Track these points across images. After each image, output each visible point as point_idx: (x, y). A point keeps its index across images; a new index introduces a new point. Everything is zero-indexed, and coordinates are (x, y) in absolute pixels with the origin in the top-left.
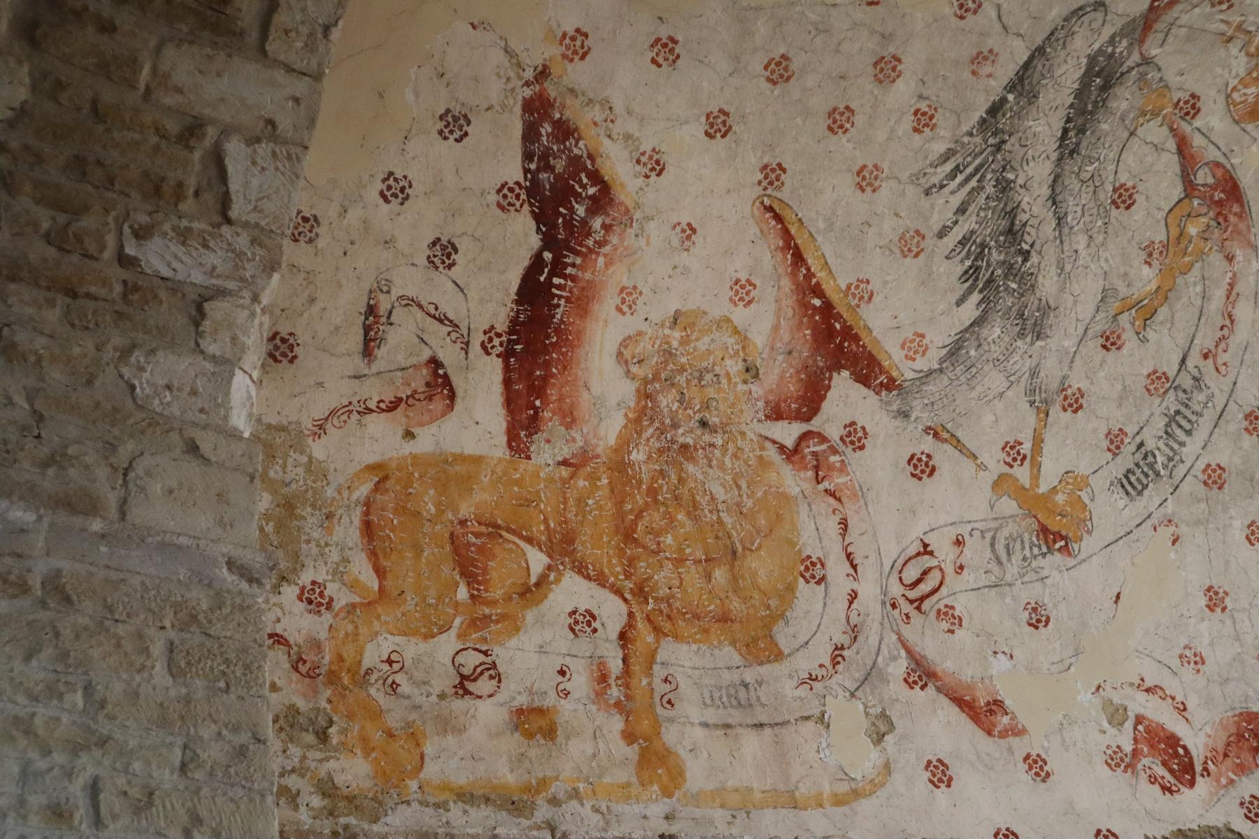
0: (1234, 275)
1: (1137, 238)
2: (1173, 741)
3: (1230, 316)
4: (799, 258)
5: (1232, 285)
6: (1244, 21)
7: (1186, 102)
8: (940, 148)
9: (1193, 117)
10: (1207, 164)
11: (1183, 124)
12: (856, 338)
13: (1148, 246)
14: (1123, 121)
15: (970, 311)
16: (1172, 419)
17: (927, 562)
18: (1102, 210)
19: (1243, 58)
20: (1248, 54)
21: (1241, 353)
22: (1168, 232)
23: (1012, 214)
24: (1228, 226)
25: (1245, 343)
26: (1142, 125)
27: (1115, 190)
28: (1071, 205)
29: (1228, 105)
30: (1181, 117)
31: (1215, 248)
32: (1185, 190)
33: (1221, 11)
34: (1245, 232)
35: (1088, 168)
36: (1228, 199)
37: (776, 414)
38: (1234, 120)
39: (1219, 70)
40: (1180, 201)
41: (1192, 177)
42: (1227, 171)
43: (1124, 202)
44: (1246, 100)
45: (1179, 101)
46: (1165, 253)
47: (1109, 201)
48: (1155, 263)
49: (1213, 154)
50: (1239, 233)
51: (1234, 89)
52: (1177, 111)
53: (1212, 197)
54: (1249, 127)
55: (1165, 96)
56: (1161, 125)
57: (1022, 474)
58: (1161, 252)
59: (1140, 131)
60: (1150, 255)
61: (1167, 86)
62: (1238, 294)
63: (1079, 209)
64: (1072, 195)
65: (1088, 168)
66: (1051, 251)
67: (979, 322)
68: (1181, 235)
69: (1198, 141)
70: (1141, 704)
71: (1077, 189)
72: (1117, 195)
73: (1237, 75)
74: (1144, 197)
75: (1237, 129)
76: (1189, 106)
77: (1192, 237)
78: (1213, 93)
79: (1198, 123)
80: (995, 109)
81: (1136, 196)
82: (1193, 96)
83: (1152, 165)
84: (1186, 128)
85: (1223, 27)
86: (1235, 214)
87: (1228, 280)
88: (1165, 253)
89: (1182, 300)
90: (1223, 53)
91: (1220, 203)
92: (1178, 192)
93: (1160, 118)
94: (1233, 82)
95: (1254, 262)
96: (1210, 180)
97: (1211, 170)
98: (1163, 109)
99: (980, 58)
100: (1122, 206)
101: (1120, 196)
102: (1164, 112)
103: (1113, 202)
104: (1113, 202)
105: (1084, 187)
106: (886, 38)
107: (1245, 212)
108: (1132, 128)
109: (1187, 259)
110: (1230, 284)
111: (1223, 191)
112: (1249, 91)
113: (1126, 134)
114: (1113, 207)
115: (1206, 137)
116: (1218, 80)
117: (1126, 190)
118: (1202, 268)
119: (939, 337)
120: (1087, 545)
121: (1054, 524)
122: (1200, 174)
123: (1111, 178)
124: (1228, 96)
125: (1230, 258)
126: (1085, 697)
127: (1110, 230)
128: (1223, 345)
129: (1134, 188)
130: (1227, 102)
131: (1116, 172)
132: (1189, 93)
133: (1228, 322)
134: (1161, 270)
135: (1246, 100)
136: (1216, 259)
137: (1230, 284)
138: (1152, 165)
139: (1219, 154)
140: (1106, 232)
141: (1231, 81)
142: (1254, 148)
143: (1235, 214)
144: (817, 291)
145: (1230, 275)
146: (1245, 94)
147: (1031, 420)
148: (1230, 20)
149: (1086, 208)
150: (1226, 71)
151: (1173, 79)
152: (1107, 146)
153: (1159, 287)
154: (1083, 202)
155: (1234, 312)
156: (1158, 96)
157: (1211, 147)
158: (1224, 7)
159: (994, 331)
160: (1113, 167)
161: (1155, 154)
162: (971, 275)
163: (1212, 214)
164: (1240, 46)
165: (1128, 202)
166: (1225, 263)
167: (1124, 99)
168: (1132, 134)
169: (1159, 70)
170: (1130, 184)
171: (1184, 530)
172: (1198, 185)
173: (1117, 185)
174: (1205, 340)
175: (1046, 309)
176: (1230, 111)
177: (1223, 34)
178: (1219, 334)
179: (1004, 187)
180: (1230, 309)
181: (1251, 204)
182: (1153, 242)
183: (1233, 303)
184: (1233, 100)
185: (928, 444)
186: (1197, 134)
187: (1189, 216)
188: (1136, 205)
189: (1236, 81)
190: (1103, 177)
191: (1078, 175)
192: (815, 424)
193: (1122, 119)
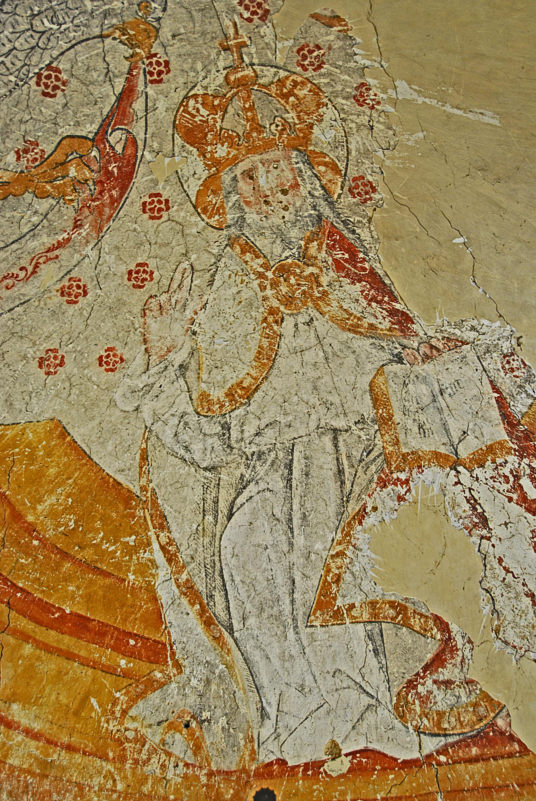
0: (69, 240)
1: (29, 126)
3: (36, 266)
5: (60, 245)
6: (247, 46)
7: (158, 63)
9: (152, 82)
10: (128, 132)
11: (142, 77)
13: (31, 143)
14: (105, 17)
18: (24, 70)
19: (221, 80)
20: (226, 78)
21: (17, 303)
22: (55, 150)
24: (98, 199)
25: (27, 298)
26: (114, 39)
27: (49, 67)
29: (181, 104)
30: (145, 69)
31: (75, 204)
32: (96, 134)
33: (241, 15)
34: (105, 217)
35: (45, 21)
36: (116, 179)
38: (175, 121)
39: (199, 66)
40: (86, 138)
41: (110, 131)
42: (136, 157)
43: (47, 86)
44: (194, 116)
45: (155, 55)
46: (37, 163)
47: (37, 71)
48: (23, 161)
49: (138, 130)
50: (101, 214)
51: (195, 96)
52: (147, 62)
53: (109, 162)
54: (179, 141)
55: (149, 37)
56: (126, 58)
58: (36, 159)
59: (108, 41)
60: (26, 151)
61: (157, 30)
62: (57, 257)
63: (9, 46)
64: (13, 27)
65: (45, 21)
68: (62, 164)
69: (138, 105)
71: (22, 28)
72: (46, 73)
73: (206, 88)
74: (65, 101)
75: (170, 132)
76: (157, 69)
77: (67, 176)
78: (181, 80)
79: (150, 90)
81: (59, 92)
82: (167, 63)
83: (92, 83)
84: (140, 87)
85: (231, 31)
86: (111, 196)
87: (60, 238)
88: (37, 163)
89: (15, 213)
90: (213, 56)
91: (109, 174)
93: (131, 51)
94: (199, 90)
95: (90, 247)
96: (119, 148)
97: (127, 139)
98: (139, 47)
100: (43, 87)
101: (48, 77)
102: (138, 51)
103: (39, 75)
104: (39, 75)
105: (28, 34)
107: (120, 203)
108: (105, 32)
109: (48, 187)
110: (59, 242)
111: (119, 168)
112: (203, 112)
113: (97, 31)
114: (35, 79)
115: (146, 110)
116: (192, 74)
117: (57, 79)
118: (52, 208)
122: (118, 134)
123: (55, 53)
124: (186, 97)
125: (77, 225)
127: (15, 94)
128: (10, 282)
129: (64, 84)
130: (183, 101)
131: (62, 54)
132: (167, 59)
133: (30, 269)
134: (22, 172)
135: (194, 116)
136: (69, 212)
137: (59, 242)
138: (92, 83)
139: (142, 136)
140: (10, 91)
141: (199, 87)
142: (167, 160)
143: (111, 196)
145: (65, 236)
146: (198, 111)
148: (240, 32)
149: (14, 51)
150: (203, 74)
151: (166, 33)
152: (76, 22)
153: (9, 183)
154: (17, 45)
155: (42, 266)
156: (145, 30)
157: (142, 122)
158: (246, 15)
160: (66, 46)
161: (102, 78)
163: (95, 175)
164: (228, 63)
165: (49, 90)
166: (71, 223)
168: (101, 37)
169: (164, 10)
170: (64, 76)
172: (108, 142)
173: (54, 65)
176: (178, 111)
177: (227, 38)
178: (16, 271)
180: (41, 261)
181: (127, 202)
182: (37, 145)
183: (49, 259)
184: (187, 105)
186: (142, 99)
187: (81, 157)
188: (52, 100)
189: (201, 92)
190: (50, 44)
191: (33, 16)
193: (106, 14)
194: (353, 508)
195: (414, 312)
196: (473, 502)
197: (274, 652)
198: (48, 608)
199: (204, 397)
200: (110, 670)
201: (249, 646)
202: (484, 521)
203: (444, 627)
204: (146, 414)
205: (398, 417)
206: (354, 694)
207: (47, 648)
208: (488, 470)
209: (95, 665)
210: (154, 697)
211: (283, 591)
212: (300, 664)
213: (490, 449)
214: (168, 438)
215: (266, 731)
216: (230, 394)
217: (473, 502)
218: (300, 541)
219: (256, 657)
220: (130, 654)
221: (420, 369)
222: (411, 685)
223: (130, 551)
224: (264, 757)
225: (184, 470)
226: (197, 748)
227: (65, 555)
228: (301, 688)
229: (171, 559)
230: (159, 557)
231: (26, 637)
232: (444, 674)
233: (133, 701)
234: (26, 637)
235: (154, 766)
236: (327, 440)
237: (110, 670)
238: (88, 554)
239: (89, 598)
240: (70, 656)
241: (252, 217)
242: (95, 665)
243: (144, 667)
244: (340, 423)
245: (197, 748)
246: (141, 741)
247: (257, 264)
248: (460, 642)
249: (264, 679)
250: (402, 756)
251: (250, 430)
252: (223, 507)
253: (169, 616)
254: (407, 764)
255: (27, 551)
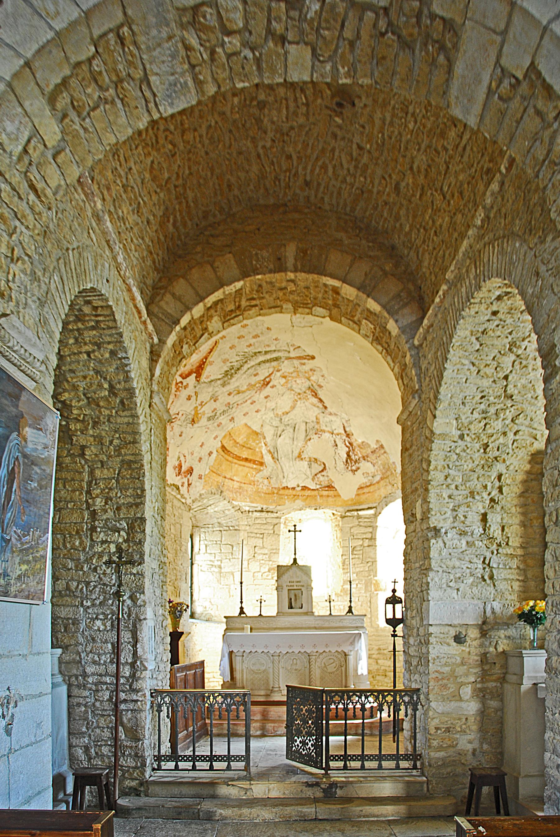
2: (181, 467)
4: (210, 353)
8: (246, 350)
12: (202, 369)
15: (220, 377)
16: (224, 411)
17: (177, 416)
23: (241, 366)
28: (249, 371)
37: (181, 376)
57: (199, 407)
66: (239, 375)
67: (219, 379)
70: (182, 458)
80: (259, 352)
92: (262, 379)
99: (268, 346)
106: (262, 333)
119: (212, 378)
120: (195, 425)
121: (196, 419)
126: (177, 453)
144: (206, 359)
147: (209, 399)
159: (219, 382)
162: (227, 371)
167: (274, 364)
171: (209, 431)
174: (239, 403)
175: (229, 383)
179: (246, 362)
185: (193, 394)
192: (184, 381)
194: (308, 438)
195: (328, 406)
196: (335, 442)
197: (287, 465)
198: (240, 457)
199: (277, 414)
200: (252, 468)
201: (282, 464)
202: (337, 445)
203: (324, 465)
204: (264, 418)
205: (321, 422)
206: (303, 475)
207: (240, 465)
208: (339, 437)
209: (249, 467)
210: (261, 473)
211: (290, 453)
212: (293, 469)
213: (340, 434)
214: (268, 421)
215: (284, 481)
216: (283, 413)
217: (335, 442)
218: (295, 443)
219: (283, 466)
220: (256, 464)
221: (328, 416)
222: (316, 475)
223: (257, 444)
224: (284, 485)
225: (270, 427)
226: (269, 483)
227: (244, 446)
228: (292, 473)
229: (266, 445)
230: (263, 445)
231: (236, 463)
232: (323, 473)
233: (257, 473)
234: (236, 463)
235: (261, 486)
236: (304, 424)
237: (252, 468)
238: (248, 446)
239: (248, 455)
240: (244, 466)
241: (294, 386)
242: (249, 467)
243: (258, 467)
244: (308, 421)
245: (269, 483)
246: (258, 481)
247: (293, 392)
248: (327, 468)
249: (285, 471)
250: (312, 488)
251: (286, 420)
252: (278, 435)
253: (265, 457)
254: (313, 490)
255: (236, 447)
